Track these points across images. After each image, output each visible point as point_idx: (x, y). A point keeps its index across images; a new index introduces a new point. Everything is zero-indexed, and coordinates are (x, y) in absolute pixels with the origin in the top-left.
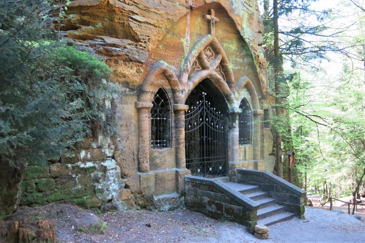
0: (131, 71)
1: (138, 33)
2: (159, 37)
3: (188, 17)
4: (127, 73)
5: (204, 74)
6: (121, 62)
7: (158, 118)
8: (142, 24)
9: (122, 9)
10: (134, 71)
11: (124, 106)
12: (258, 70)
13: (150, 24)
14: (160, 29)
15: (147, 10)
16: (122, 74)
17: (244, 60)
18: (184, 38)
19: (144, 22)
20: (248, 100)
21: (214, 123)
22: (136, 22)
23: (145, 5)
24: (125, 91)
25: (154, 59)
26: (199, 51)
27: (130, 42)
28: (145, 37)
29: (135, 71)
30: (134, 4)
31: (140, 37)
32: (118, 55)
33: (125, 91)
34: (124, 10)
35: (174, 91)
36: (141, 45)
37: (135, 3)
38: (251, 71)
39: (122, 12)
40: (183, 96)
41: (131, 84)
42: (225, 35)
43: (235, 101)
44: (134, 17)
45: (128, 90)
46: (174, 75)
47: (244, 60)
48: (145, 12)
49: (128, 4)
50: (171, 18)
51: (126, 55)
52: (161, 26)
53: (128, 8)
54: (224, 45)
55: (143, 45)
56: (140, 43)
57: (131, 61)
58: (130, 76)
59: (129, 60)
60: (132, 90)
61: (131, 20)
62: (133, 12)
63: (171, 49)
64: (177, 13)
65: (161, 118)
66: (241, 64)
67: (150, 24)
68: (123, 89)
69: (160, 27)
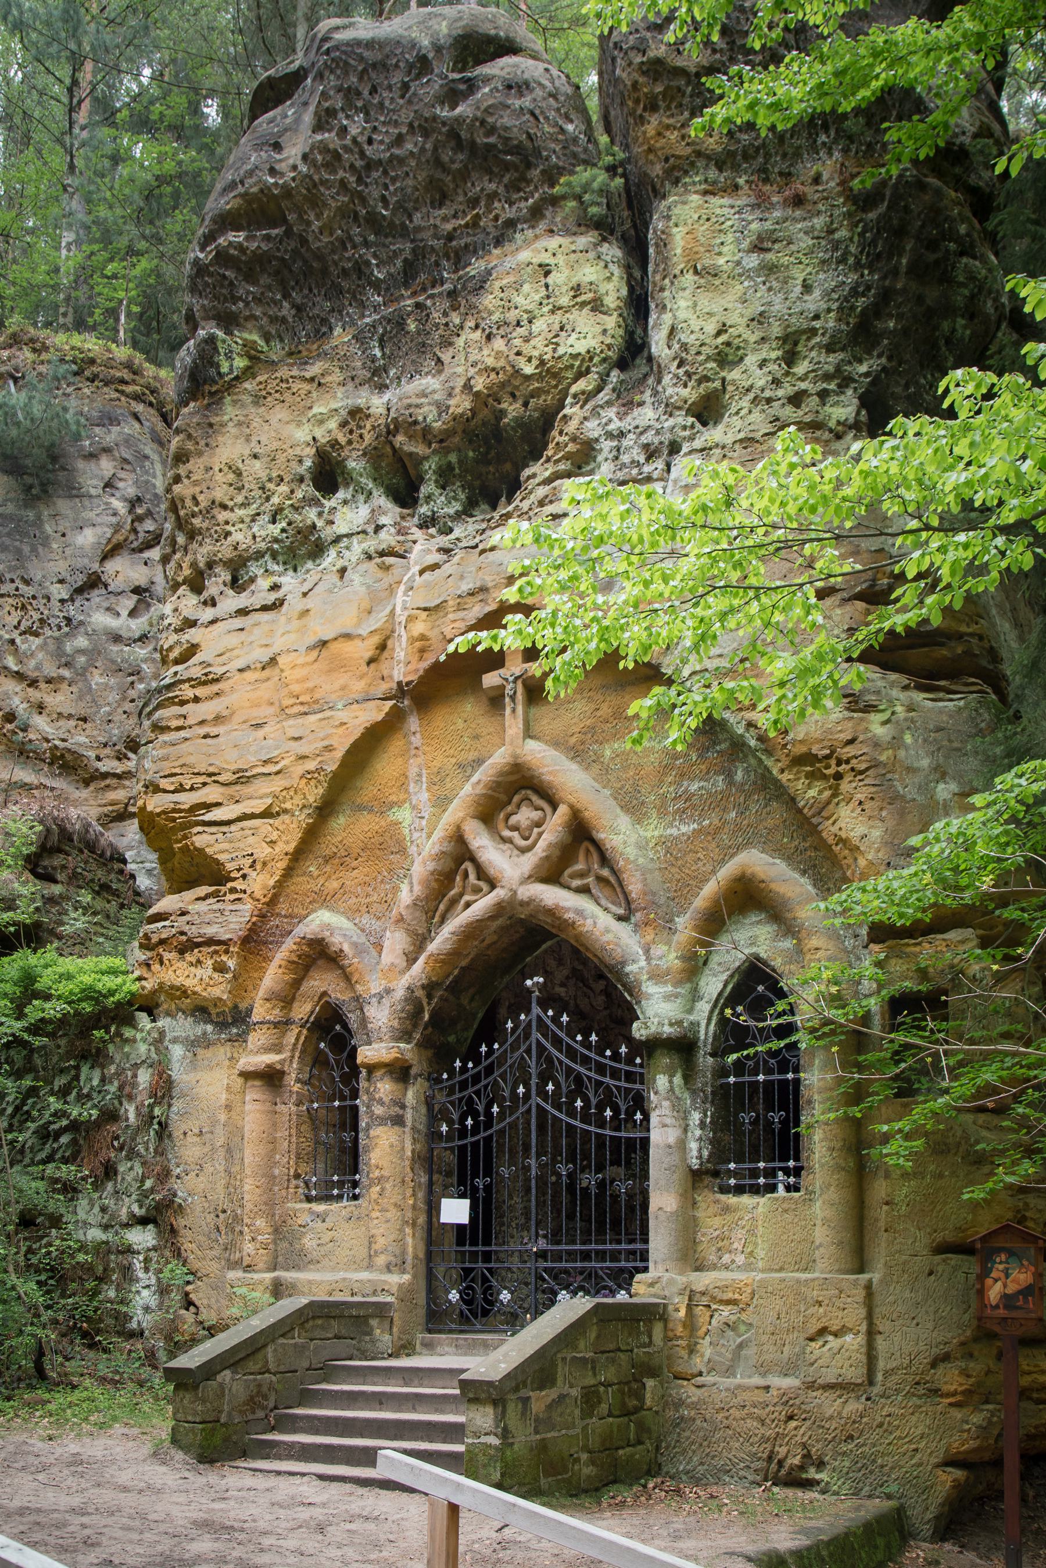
0: (199, 972)
1: (222, 857)
2: (287, 842)
3: (413, 723)
4: (188, 983)
5: (482, 905)
6: (167, 956)
7: (761, 1077)
8: (233, 828)
9: (174, 811)
10: (206, 971)
11: (199, 1075)
12: (811, 793)
13: (253, 816)
14: (286, 818)
15: (242, 778)
16: (178, 989)
17: (730, 776)
18: (399, 804)
19: (239, 819)
20: (777, 963)
21: (586, 1100)
22: (213, 829)
23: (234, 767)
24: (205, 1033)
25: (291, 916)
26: (451, 829)
27: (203, 890)
28: (242, 861)
29: (210, 971)
30: (209, 780)
31: (230, 866)
32: (162, 942)
33: (205, 1033)
34: (180, 811)
35: (359, 1003)
36: (233, 890)
37: (210, 775)
38: (777, 813)
39: (174, 820)
40: (381, 1016)
41: (214, 1011)
42: (605, 710)
43: (650, 988)
44: (208, 817)
45: (209, 1028)
46: (346, 947)
47: (730, 776)
48: (238, 787)
49: (192, 789)
50: (311, 765)
51: (182, 933)
52: (288, 805)
53: (187, 799)
54: (608, 753)
55: (239, 885)
56: (229, 885)
57: (198, 945)
58: (198, 989)
59: (187, 946)
60: (222, 1025)
61: (200, 829)
62: (208, 806)
63: (355, 863)
64: (334, 742)
65: (776, 1077)
66: (718, 803)
67: (253, 816)
68: (199, 1030)
69: (285, 811)
